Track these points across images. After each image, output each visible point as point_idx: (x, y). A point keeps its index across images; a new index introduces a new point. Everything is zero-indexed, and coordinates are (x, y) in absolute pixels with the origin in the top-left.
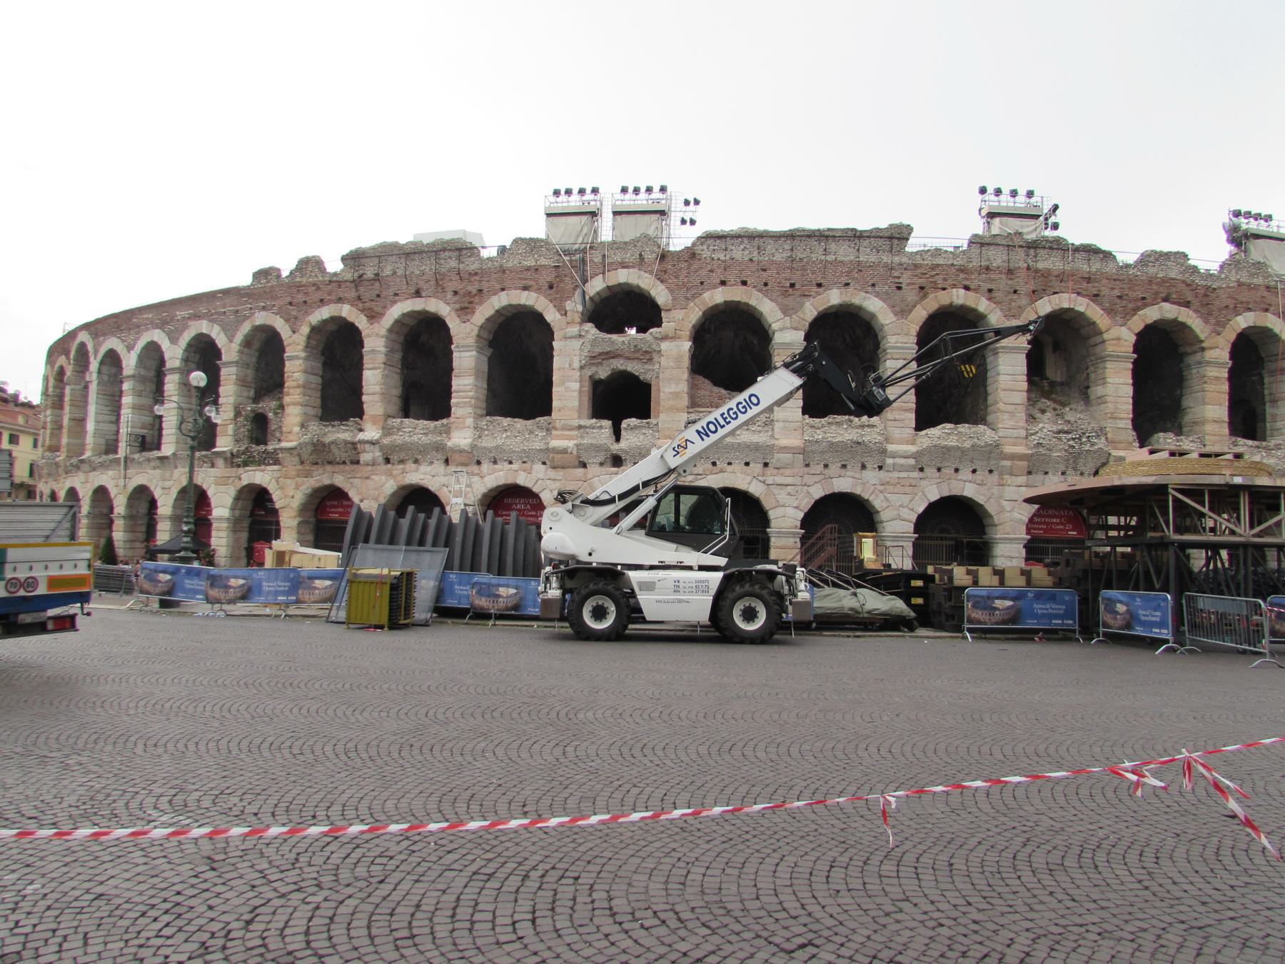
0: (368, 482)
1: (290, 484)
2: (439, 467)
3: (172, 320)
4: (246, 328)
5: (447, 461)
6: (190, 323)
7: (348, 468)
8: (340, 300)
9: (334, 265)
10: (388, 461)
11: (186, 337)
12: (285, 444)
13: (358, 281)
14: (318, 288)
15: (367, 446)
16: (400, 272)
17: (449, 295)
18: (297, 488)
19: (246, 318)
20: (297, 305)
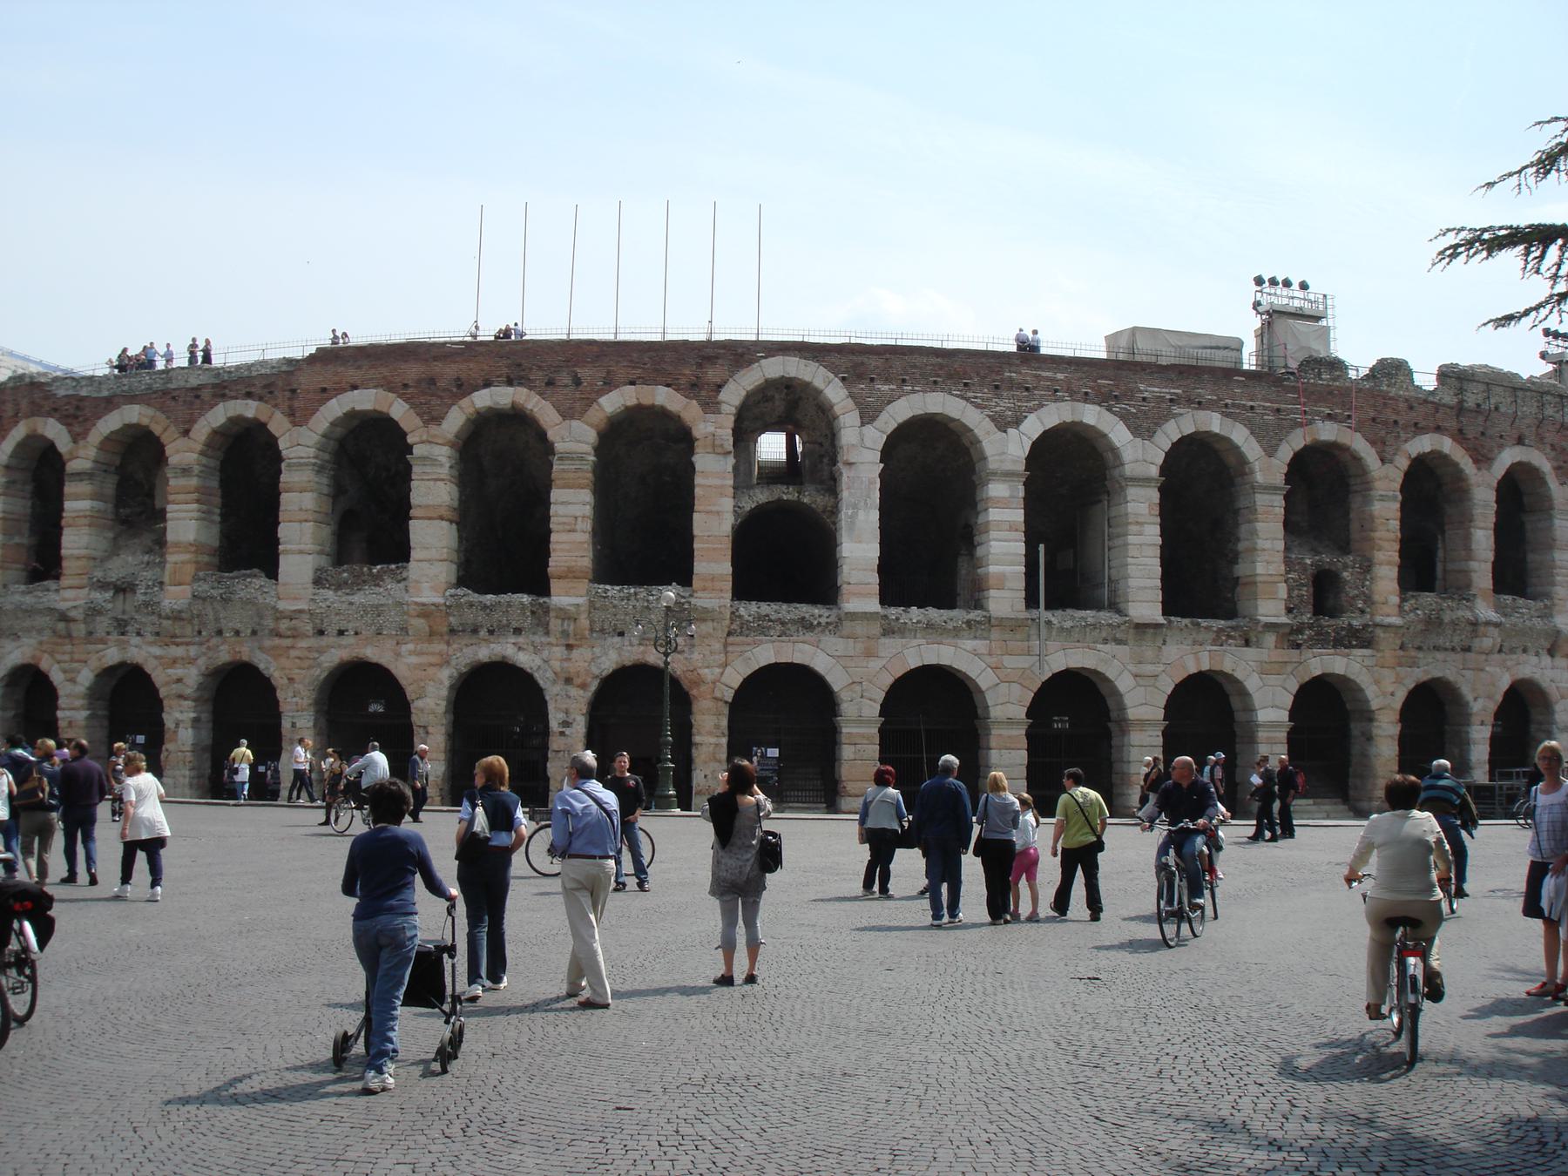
0: (1483, 675)
1: (1388, 676)
2: (1546, 660)
3: (1129, 395)
4: (1297, 441)
5: (1551, 652)
6: (1176, 410)
7: (1459, 656)
8: (1438, 429)
9: (1426, 380)
10: (1500, 651)
11: (1171, 432)
12: (1378, 619)
13: (1460, 409)
14: (1411, 408)
15: (1491, 629)
16: (1502, 409)
17: (1548, 450)
18: (1399, 681)
19: (1297, 425)
20: (1385, 423)
